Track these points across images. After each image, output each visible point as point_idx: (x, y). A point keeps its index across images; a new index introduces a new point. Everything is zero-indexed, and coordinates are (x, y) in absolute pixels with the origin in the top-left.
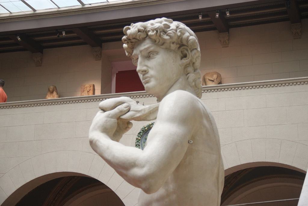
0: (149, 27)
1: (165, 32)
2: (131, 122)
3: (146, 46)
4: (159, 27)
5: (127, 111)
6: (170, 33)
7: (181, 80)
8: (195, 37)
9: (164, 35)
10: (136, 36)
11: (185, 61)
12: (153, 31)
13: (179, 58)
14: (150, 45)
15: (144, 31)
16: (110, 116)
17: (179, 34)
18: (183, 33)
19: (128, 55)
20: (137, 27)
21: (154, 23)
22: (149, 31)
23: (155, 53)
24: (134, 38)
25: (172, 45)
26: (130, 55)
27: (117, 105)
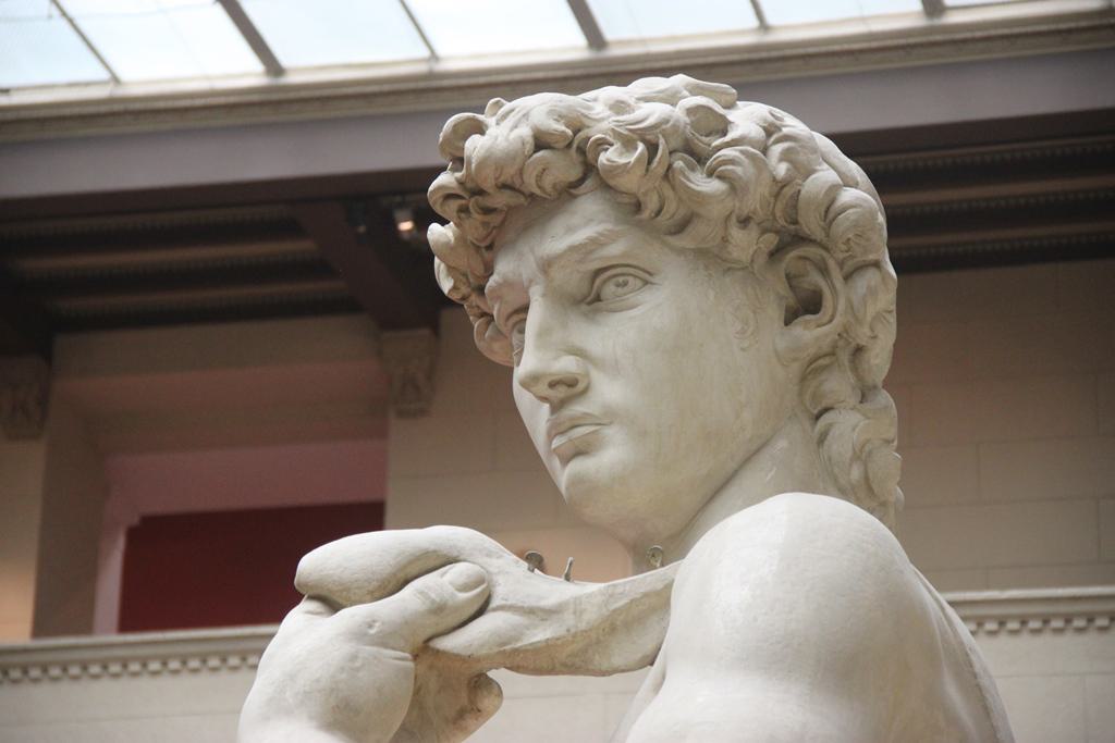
0: (598, 121)
1: (698, 157)
2: (490, 682)
3: (581, 236)
4: (667, 121)
5: (475, 607)
6: (732, 161)
7: (782, 444)
8: (874, 197)
9: (693, 169)
10: (521, 172)
11: (811, 334)
12: (628, 144)
13: (775, 313)
14: (610, 226)
15: (569, 145)
16: (372, 631)
17: (782, 169)
18: (803, 171)
19: (455, 288)
20: (526, 116)
21: (632, 101)
22: (602, 144)
23: (635, 277)
24: (505, 186)
25: (737, 234)
26: (464, 290)
27: (413, 570)
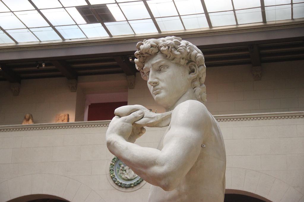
0: (161, 43)
1: (176, 49)
2: (144, 128)
3: (158, 61)
4: (171, 43)
6: (181, 49)
7: (188, 92)
9: (175, 50)
10: (149, 51)
11: (193, 76)
12: (165, 47)
13: (187, 72)
16: (126, 121)
17: (189, 51)
18: (192, 51)
19: (139, 69)
20: (149, 42)
21: (166, 40)
22: (161, 47)
24: (146, 53)
25: (182, 60)
26: (140, 69)
27: (132, 112)
